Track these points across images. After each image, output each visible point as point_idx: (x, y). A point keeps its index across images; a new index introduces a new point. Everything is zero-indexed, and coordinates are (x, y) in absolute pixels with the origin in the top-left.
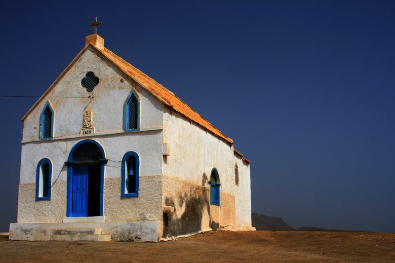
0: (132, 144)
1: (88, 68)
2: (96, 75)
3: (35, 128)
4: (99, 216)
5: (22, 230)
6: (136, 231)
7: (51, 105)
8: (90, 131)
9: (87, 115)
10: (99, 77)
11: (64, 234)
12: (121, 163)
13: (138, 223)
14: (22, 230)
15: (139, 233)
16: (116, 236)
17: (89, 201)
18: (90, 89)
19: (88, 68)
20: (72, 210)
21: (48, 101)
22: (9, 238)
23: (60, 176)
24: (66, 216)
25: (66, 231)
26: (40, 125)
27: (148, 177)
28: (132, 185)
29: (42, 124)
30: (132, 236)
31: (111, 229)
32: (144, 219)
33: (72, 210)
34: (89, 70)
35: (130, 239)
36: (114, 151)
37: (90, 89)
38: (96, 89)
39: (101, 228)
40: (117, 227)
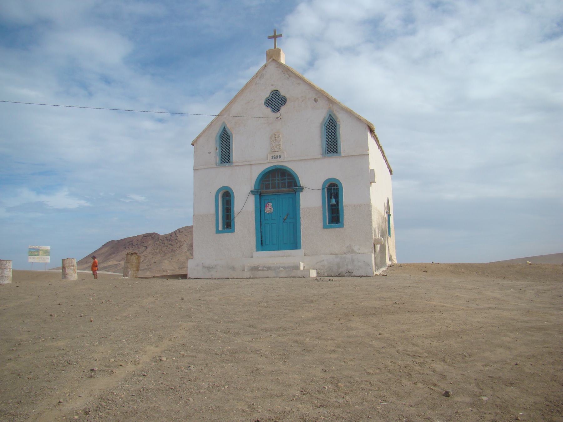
0: (332, 169)
1: (272, 85)
2: (282, 93)
3: (210, 153)
4: (297, 249)
5: (203, 267)
6: (347, 265)
7: (229, 126)
8: (280, 157)
9: (275, 137)
10: (287, 96)
11: (263, 270)
12: (320, 191)
13: (349, 256)
14: (203, 267)
15: (350, 267)
16: (322, 271)
17: (278, 232)
18: (276, 109)
19: (272, 85)
20: (263, 243)
21: (224, 122)
22: (188, 276)
23: (245, 206)
24: (255, 250)
25: (264, 267)
26: (217, 149)
27: (355, 205)
28: (334, 215)
29: (218, 147)
30: (342, 270)
31: (317, 263)
32: (352, 252)
33: (263, 243)
34: (273, 88)
35: (339, 274)
36: (312, 179)
37: (276, 109)
38: (283, 109)
39: (306, 260)
40: (323, 261)
